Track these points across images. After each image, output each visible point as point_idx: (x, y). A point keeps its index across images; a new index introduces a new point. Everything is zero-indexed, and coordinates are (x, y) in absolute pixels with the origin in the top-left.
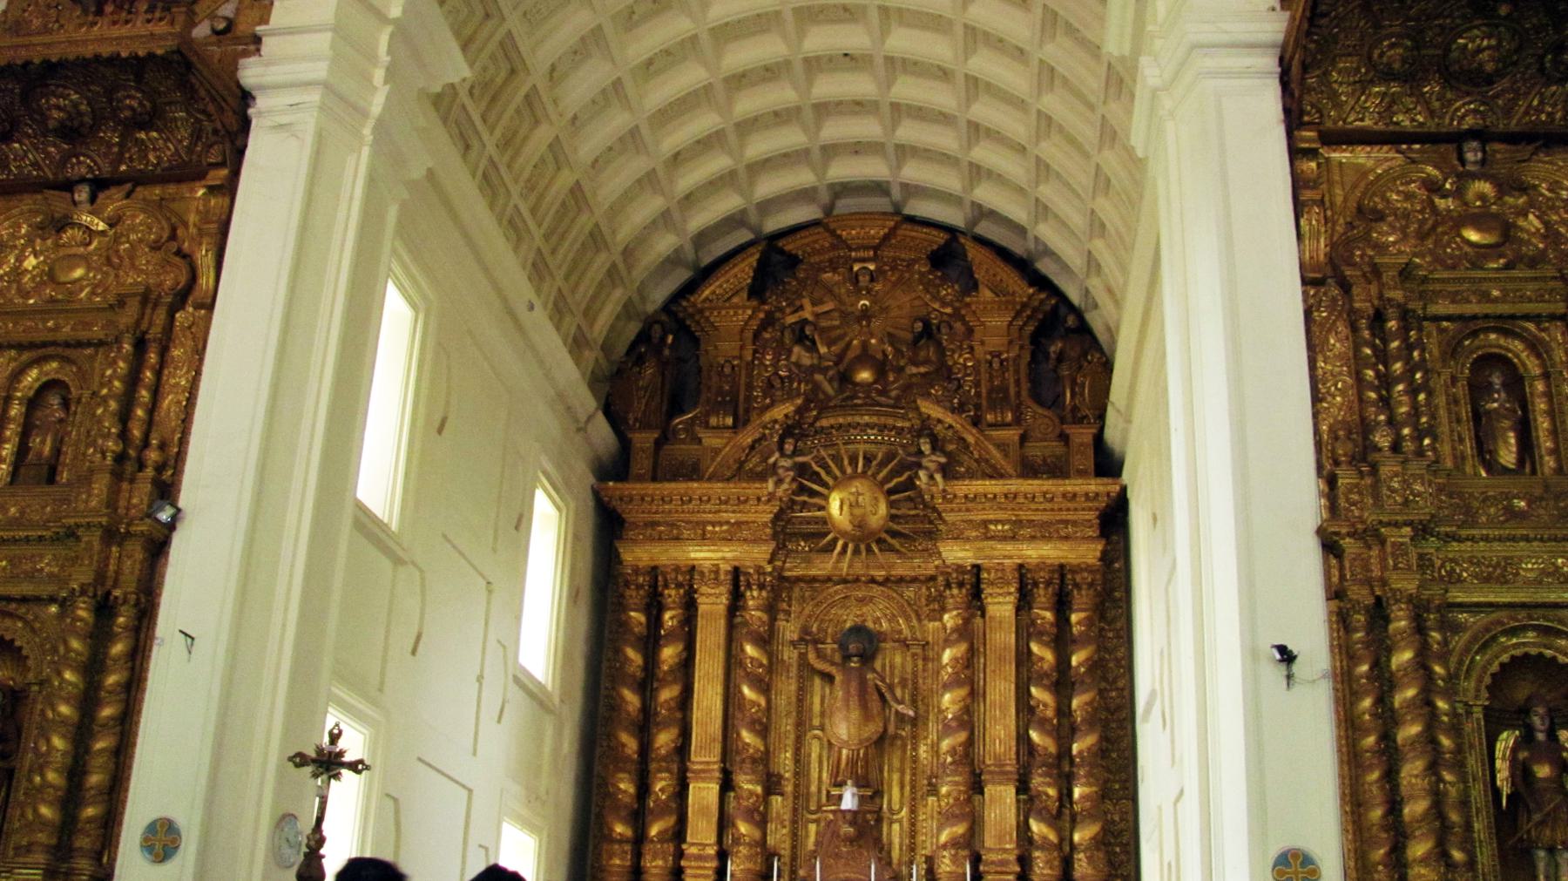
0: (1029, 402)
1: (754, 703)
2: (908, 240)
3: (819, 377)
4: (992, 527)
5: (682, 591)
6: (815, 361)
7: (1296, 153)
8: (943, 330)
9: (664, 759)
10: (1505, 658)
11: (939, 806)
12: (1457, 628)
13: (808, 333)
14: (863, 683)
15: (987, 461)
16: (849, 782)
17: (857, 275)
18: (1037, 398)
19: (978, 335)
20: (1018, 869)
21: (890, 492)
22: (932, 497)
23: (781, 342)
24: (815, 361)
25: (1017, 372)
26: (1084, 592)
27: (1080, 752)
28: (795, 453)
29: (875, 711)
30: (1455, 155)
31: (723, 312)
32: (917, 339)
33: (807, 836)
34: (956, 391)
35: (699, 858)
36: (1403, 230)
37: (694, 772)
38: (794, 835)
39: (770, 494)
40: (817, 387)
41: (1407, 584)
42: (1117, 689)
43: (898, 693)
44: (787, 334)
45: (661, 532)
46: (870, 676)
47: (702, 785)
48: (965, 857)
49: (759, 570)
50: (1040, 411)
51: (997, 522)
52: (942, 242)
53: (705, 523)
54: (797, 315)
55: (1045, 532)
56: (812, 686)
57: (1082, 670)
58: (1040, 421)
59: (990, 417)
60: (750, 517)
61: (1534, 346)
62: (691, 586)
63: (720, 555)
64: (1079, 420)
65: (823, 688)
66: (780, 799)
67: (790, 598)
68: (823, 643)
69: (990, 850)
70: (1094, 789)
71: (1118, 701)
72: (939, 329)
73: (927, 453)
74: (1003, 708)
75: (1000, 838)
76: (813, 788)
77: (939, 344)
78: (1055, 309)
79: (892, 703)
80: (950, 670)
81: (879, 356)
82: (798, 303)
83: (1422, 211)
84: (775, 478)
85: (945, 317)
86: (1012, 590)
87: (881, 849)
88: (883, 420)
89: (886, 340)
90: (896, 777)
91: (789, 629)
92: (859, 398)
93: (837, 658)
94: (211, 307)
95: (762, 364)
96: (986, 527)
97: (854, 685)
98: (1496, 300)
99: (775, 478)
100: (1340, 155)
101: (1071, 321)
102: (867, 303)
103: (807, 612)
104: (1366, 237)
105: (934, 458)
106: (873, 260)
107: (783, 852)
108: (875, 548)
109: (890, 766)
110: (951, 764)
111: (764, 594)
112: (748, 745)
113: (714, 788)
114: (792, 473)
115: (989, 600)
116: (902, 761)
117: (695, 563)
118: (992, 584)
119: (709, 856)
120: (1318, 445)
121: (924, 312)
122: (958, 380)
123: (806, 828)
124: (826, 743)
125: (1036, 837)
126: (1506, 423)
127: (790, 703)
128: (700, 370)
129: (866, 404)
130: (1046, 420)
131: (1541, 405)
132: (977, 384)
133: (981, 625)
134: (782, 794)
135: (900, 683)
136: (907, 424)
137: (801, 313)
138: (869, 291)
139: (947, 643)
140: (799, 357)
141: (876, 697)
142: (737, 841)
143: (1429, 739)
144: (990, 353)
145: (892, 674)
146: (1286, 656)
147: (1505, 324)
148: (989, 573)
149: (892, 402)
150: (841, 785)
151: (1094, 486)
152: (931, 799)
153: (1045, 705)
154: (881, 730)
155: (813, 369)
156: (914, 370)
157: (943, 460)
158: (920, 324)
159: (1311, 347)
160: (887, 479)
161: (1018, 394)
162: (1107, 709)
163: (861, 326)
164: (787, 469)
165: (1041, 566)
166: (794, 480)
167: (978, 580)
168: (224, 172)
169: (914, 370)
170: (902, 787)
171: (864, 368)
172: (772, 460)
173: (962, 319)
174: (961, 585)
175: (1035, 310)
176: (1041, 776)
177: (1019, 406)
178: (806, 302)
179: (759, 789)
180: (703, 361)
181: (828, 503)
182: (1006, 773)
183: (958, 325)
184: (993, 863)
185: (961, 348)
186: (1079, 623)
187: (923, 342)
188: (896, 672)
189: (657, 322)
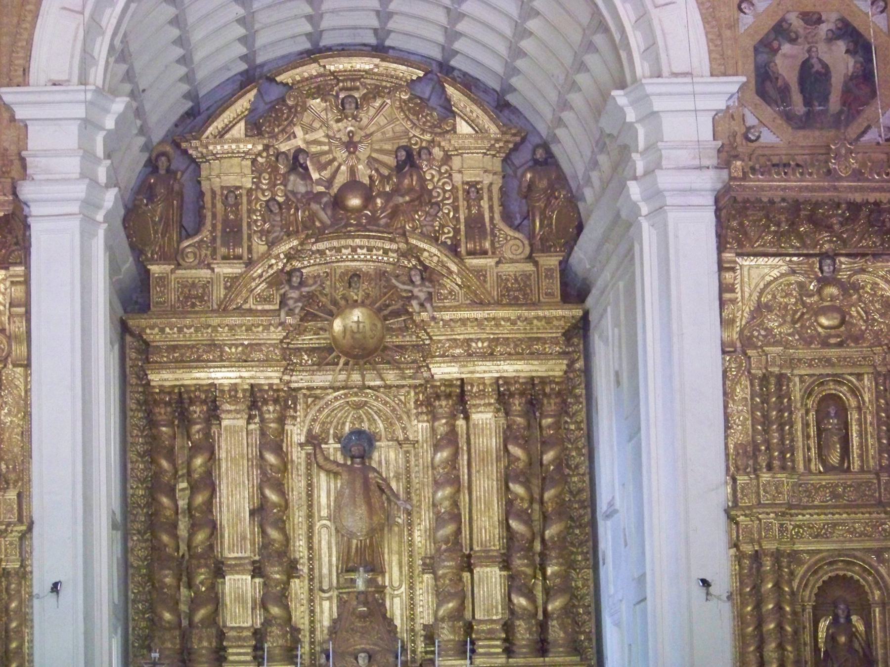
0: (501, 225)
1: (275, 505)
3: (315, 207)
5: (205, 408)
7: (721, 268)
8: (424, 157)
10: (825, 578)
12: (800, 563)
13: (302, 161)
14: (366, 482)
16: (361, 569)
17: (343, 99)
18: (507, 217)
19: (456, 162)
20: (504, 636)
23: (275, 169)
25: (490, 199)
26: (552, 401)
27: (552, 537)
28: (302, 284)
30: (818, 265)
32: (399, 168)
33: (322, 612)
35: (240, 638)
36: (783, 317)
37: (229, 566)
38: (312, 612)
40: (313, 216)
41: (770, 546)
42: (578, 474)
46: (371, 475)
47: (237, 577)
48: (460, 628)
50: (511, 233)
56: (319, 481)
57: (552, 468)
58: (511, 242)
59: (470, 246)
61: (854, 391)
62: (214, 401)
64: (546, 250)
65: (328, 483)
66: (297, 581)
68: (326, 443)
69: (480, 622)
70: (563, 568)
71: (580, 485)
72: (419, 154)
74: (488, 505)
75: (488, 612)
76: (325, 571)
79: (392, 498)
80: (441, 471)
81: (366, 181)
83: (795, 304)
84: (286, 309)
85: (424, 144)
86: (492, 401)
87: (390, 622)
88: (373, 243)
90: (395, 558)
91: (296, 433)
92: (351, 225)
93: (340, 459)
94: (28, 366)
95: (258, 187)
96: (469, 346)
97: (358, 485)
98: (833, 365)
100: (746, 262)
102: (352, 129)
103: (310, 417)
104: (762, 324)
105: (425, 289)
107: (302, 627)
109: (390, 549)
110: (445, 551)
112: (274, 540)
114: (300, 304)
116: (400, 542)
117: (216, 382)
120: (727, 455)
122: (437, 204)
123: (321, 605)
124: (333, 532)
125: (516, 609)
126: (835, 439)
127: (300, 498)
128: (202, 194)
129: (358, 231)
130: (517, 242)
131: (855, 428)
132: (456, 209)
135: (394, 476)
136: (394, 246)
137: (293, 141)
139: (437, 447)
141: (378, 493)
143: (780, 627)
144: (468, 183)
145: (388, 469)
146: (705, 583)
147: (838, 380)
148: (472, 386)
150: (353, 570)
153: (522, 499)
156: (401, 200)
158: (404, 153)
159: (725, 394)
161: (492, 219)
162: (571, 492)
164: (297, 300)
165: (516, 380)
166: (302, 309)
167: (463, 392)
168: (20, 269)
169: (401, 200)
170: (401, 567)
171: (356, 197)
173: (442, 148)
174: (448, 396)
176: (519, 558)
177: (494, 235)
178: (298, 131)
179: (285, 578)
180: (205, 186)
183: (437, 152)
184: (483, 631)
186: (549, 427)
187: (407, 169)
188: (391, 467)
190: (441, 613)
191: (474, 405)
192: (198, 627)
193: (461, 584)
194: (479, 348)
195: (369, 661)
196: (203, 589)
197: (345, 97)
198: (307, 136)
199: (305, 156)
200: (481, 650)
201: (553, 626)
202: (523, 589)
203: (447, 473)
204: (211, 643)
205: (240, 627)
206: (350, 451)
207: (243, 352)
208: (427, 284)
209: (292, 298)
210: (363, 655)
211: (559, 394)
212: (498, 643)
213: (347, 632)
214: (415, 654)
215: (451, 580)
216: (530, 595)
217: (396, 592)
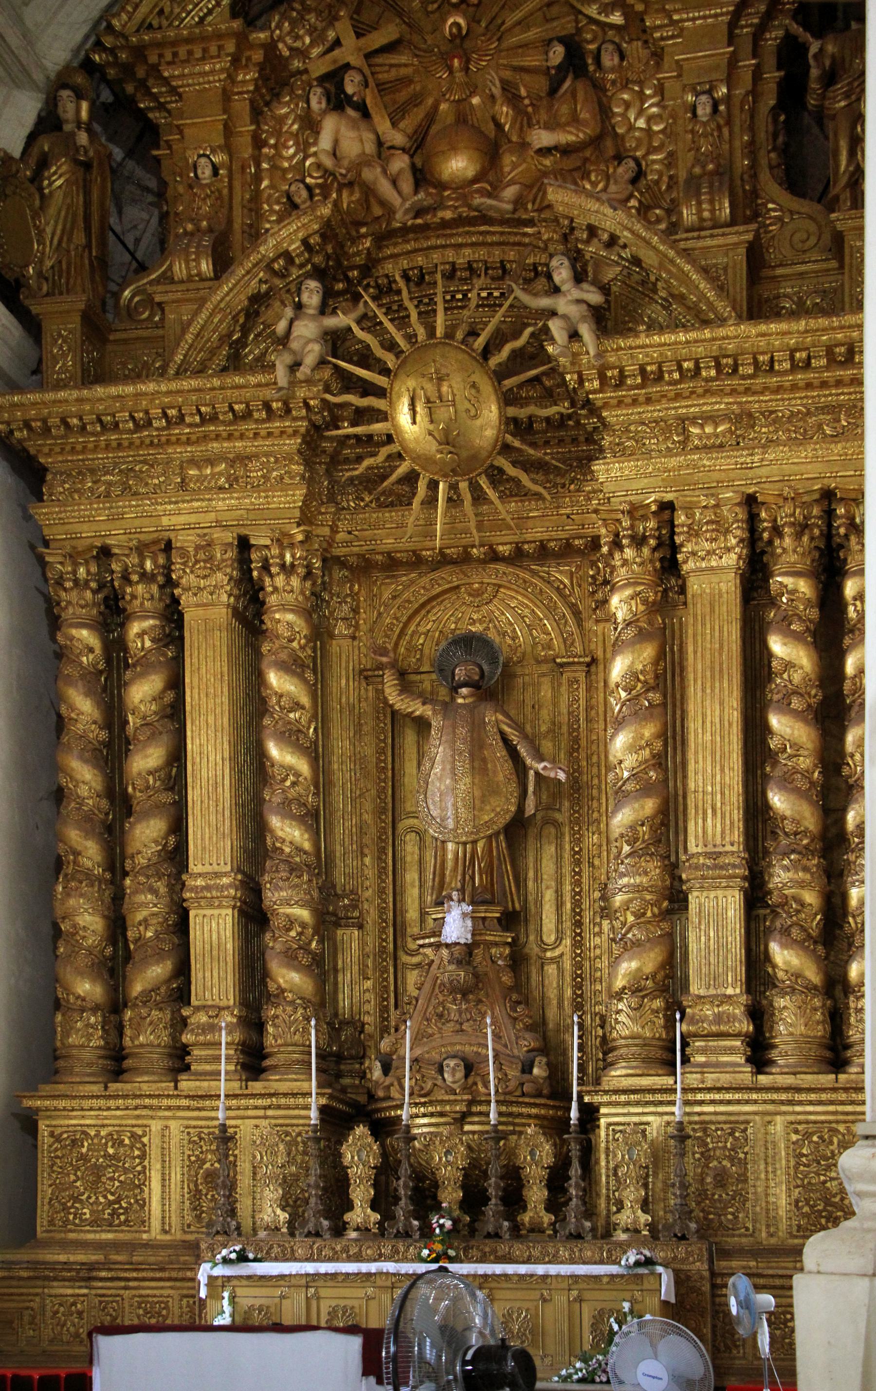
4: (695, 430)
14: (477, 727)
20: (747, 1027)
29: (501, 777)
49: (282, 541)
54: (329, 57)
63: (212, 516)
75: (715, 979)
77: (598, 87)
80: (623, 694)
89: (497, 91)
97: (462, 731)
102: (461, 21)
108: (483, 482)
116: (559, 858)
121: (570, 28)
163: (450, 69)
191: (694, 554)
194: (708, 437)
199: (358, 78)
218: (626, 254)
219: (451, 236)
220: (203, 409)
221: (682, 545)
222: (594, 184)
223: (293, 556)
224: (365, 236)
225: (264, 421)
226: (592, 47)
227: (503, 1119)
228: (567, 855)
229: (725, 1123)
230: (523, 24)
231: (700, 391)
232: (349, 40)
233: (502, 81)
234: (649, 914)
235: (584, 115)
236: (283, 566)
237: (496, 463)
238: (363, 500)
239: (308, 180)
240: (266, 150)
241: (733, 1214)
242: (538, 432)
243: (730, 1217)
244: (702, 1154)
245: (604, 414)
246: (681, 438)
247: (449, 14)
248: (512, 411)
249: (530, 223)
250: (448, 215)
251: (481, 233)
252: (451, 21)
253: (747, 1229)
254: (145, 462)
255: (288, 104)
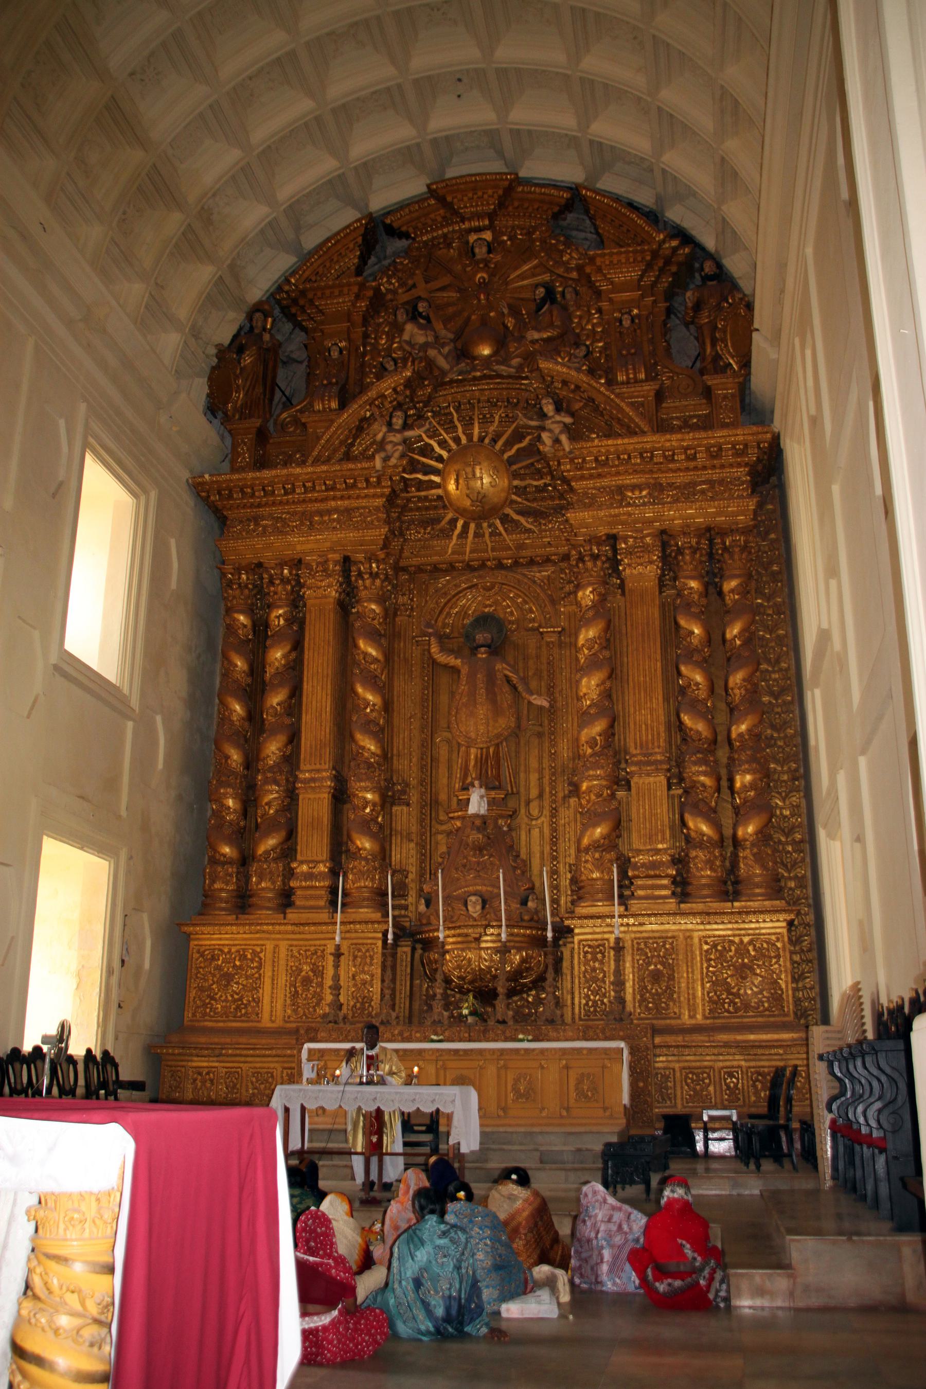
2: (526, 205)
6: (431, 339)
9: (271, 768)
11: (581, 805)
13: (421, 310)
15: (619, 419)
16: (476, 783)
21: (511, 462)
22: (559, 464)
24: (431, 339)
26: (736, 557)
28: (406, 426)
31: (328, 292)
34: (585, 356)
35: (310, 876)
39: (378, 471)
40: (431, 364)
43: (534, 684)
44: (401, 316)
45: (265, 527)
46: (498, 666)
51: (633, 488)
52: (563, 202)
53: (313, 515)
55: (687, 493)
57: (738, 642)
60: (363, 502)
66: (405, 808)
67: (411, 591)
70: (758, 776)
73: (551, 414)
76: (443, 797)
77: (565, 308)
78: (691, 258)
79: (524, 694)
80: (586, 652)
82: (410, 282)
89: (506, 311)
99: (383, 455)
101: (709, 268)
102: (485, 275)
105: (558, 418)
106: (491, 227)
110: (591, 756)
111: (378, 582)
113: (325, 797)
114: (400, 448)
115: (628, 571)
117: (301, 556)
118: (631, 553)
119: (320, 873)
122: (587, 347)
129: (484, 377)
133: (622, 604)
134: (408, 805)
135: (534, 674)
137: (413, 291)
138: (486, 262)
140: (412, 336)
141: (506, 688)
142: (355, 855)
149: (513, 370)
151: (741, 435)
152: (573, 801)
154: (513, 725)
155: (426, 346)
156: (536, 336)
157: (568, 420)
158: (542, 290)
160: (509, 444)
163: (479, 300)
164: (396, 444)
166: (403, 456)
169: (536, 336)
172: (379, 436)
175: (668, 262)
181: (444, 479)
182: (656, 762)
185: (589, 311)
189: (258, 310)
190: (586, 841)
191: (629, 565)
192: (260, 861)
193: (615, 803)
195: (483, 908)
196: (272, 812)
197: (476, 241)
198: (429, 285)
199: (425, 304)
200: (640, 893)
201: (745, 858)
202: (701, 805)
203: (593, 654)
204: (274, 883)
205: (312, 861)
206: (474, 640)
207: (338, 521)
208: (563, 414)
209: (391, 442)
210: (473, 898)
211: (745, 548)
212: (665, 882)
213: (457, 869)
214: (559, 905)
215: (599, 795)
216: (711, 815)
217: (534, 822)
218: (585, 395)
219: (479, 385)
220: (328, 482)
221: (622, 560)
222: (563, 359)
223: (378, 567)
224: (428, 385)
225: (364, 489)
226: (560, 289)
227: (512, 938)
228: (546, 755)
229: (659, 938)
230: (522, 277)
231: (631, 471)
232: (421, 285)
233: (508, 305)
234: (605, 794)
235: (558, 323)
236: (371, 574)
237: (506, 512)
238: (419, 533)
239: (394, 355)
240: (369, 340)
241: (665, 1003)
242: (529, 493)
243: (663, 1005)
244: (644, 960)
245: (573, 484)
246: (619, 498)
247: (477, 272)
248: (516, 483)
249: (526, 378)
250: (478, 374)
251: (496, 383)
252: (479, 276)
253: (675, 1013)
254: (288, 513)
255: (383, 317)
